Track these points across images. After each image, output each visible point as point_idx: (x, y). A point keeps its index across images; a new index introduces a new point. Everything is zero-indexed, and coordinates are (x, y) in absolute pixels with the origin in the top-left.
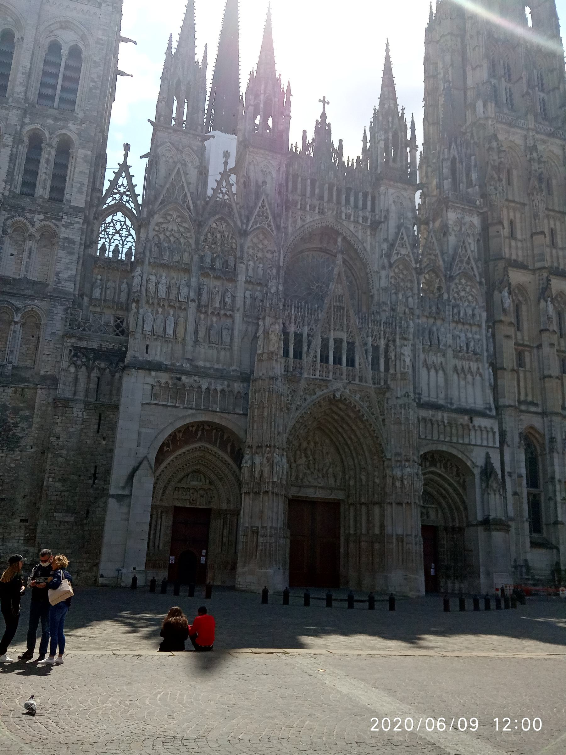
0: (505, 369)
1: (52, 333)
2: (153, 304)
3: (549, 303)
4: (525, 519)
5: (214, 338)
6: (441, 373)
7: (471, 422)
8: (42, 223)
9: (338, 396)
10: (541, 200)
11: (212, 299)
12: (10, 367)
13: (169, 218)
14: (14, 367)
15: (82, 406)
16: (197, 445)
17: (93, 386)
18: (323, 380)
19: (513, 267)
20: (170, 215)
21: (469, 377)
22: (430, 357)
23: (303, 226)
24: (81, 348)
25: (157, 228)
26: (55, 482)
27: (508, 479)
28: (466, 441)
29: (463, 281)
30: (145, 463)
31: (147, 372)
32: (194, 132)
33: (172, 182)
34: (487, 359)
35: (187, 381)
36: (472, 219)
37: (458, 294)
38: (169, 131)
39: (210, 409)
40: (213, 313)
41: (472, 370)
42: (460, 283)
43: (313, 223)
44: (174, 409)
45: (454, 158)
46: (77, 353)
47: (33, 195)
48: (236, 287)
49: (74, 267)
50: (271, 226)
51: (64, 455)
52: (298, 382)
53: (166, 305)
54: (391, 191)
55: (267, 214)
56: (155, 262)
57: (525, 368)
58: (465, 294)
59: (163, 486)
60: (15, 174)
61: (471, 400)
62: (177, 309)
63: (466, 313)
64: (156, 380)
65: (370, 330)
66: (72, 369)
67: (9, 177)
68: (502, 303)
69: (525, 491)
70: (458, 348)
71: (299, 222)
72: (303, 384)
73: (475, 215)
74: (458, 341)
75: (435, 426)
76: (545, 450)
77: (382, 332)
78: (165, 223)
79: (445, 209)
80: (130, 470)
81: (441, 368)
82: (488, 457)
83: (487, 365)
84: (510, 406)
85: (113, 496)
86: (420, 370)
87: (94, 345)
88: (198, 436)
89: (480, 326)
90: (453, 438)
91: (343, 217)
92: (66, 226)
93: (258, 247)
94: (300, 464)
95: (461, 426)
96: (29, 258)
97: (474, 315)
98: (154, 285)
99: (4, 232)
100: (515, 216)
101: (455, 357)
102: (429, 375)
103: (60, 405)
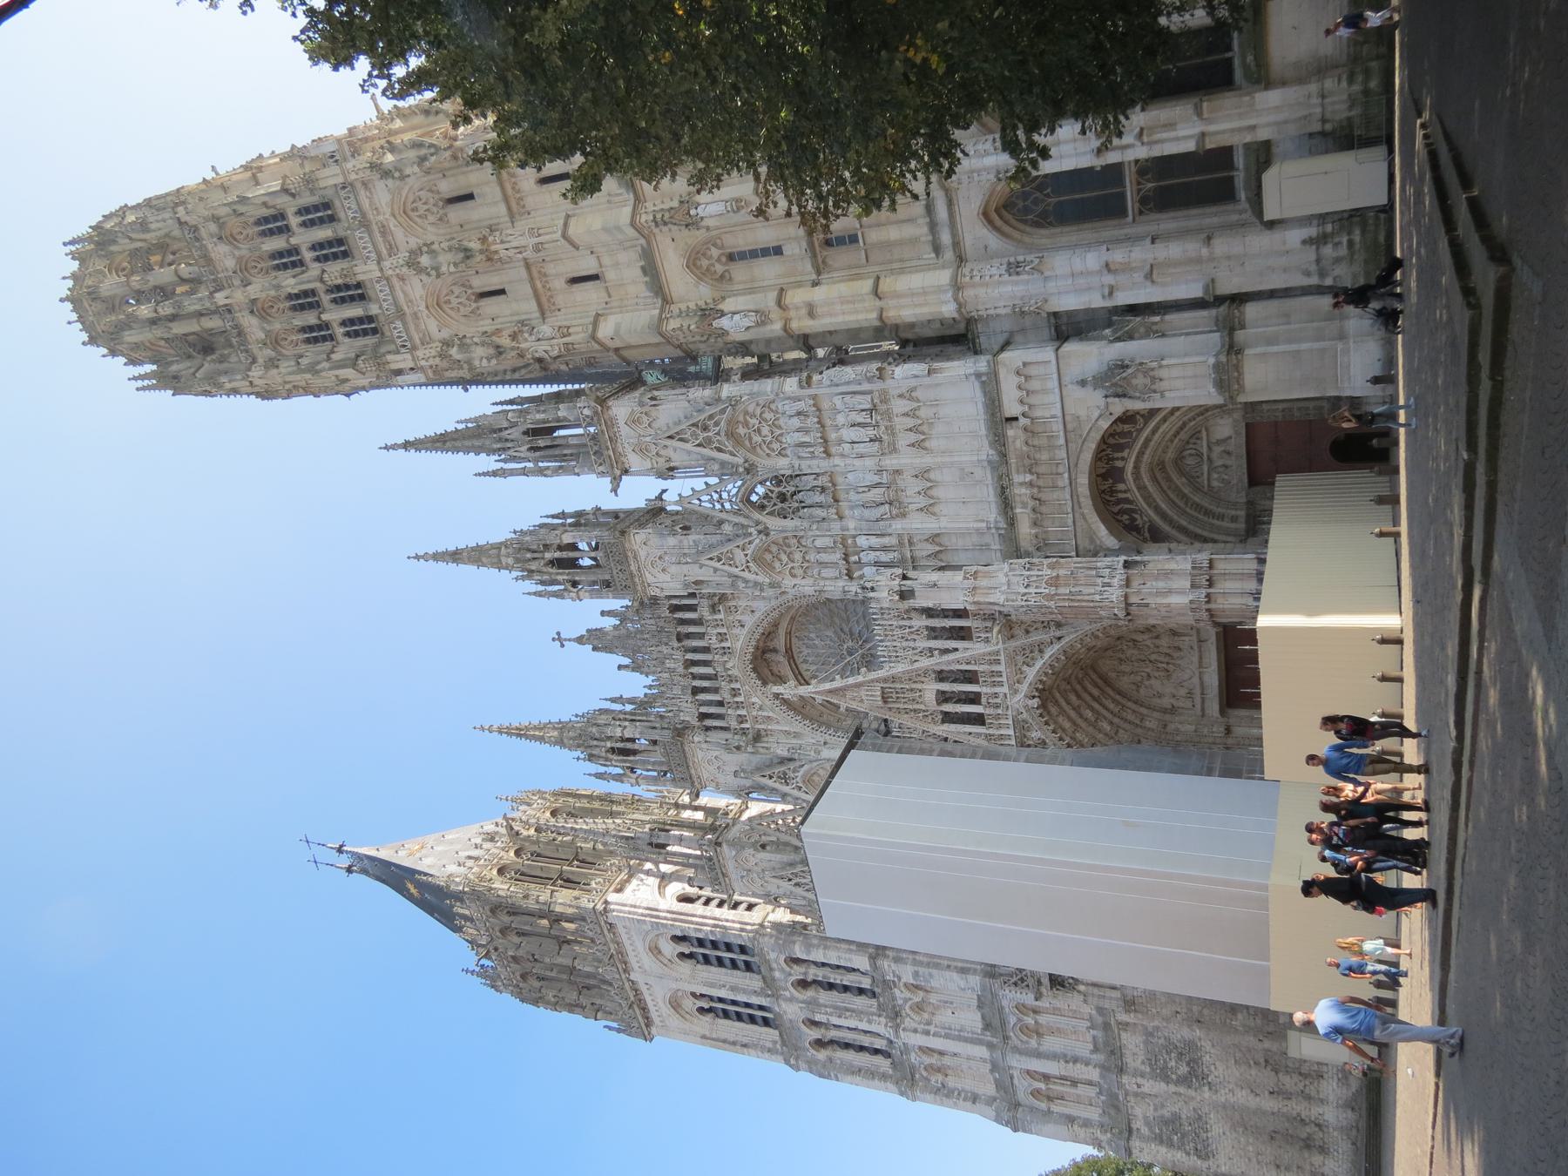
0: (882, 310)
10: (502, 242)
12: (1095, 1032)
22: (910, 500)
28: (1057, 427)
29: (741, 431)
37: (771, 442)
41: (907, 409)
43: (759, 693)
45: (531, 449)
49: (948, 974)
54: (649, 578)
65: (905, 644)
74: (860, 448)
81: (926, 475)
82: (1083, 383)
83: (889, 382)
86: (943, 525)
89: (814, 397)
97: (799, 414)
99: (929, 1023)
101: (893, 449)
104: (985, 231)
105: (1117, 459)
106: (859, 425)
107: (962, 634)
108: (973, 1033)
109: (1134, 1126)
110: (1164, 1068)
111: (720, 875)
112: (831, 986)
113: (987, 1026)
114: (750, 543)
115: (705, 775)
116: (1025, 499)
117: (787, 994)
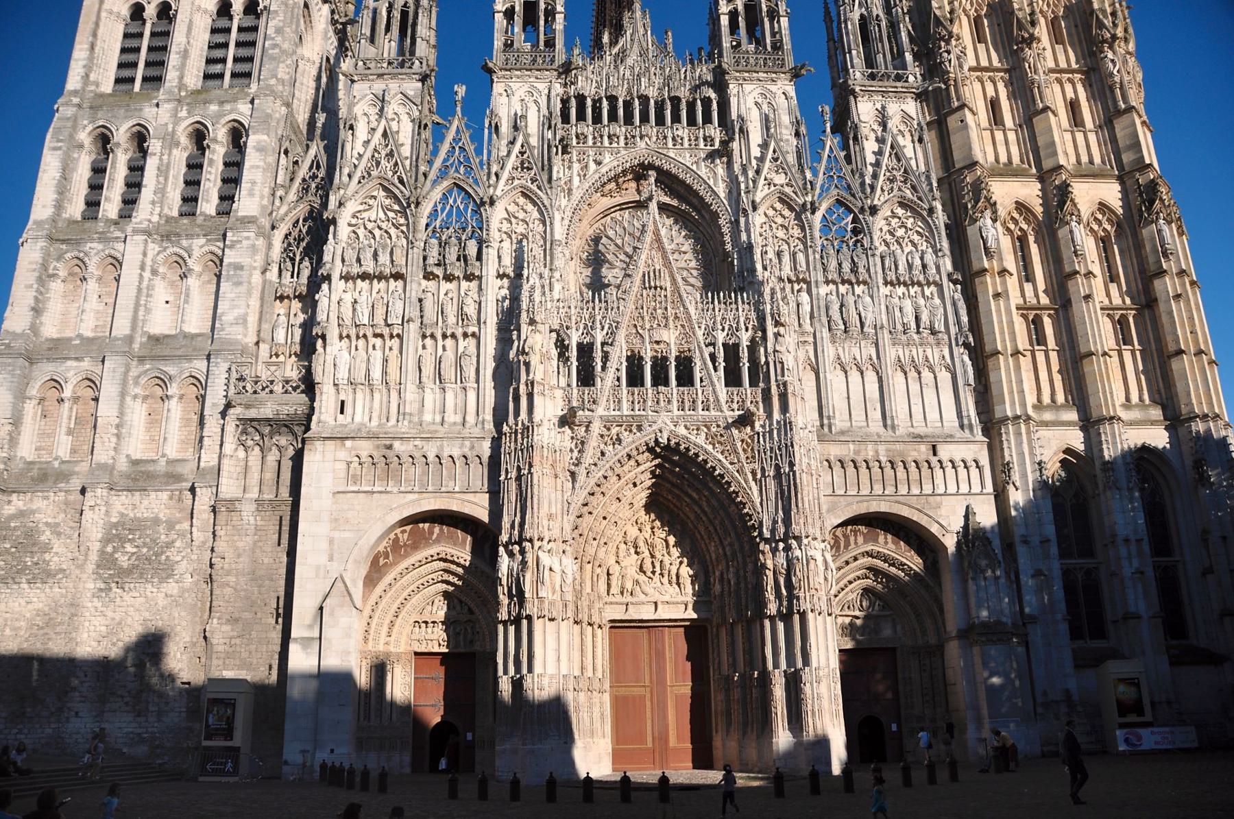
1: (214, 405)
2: (348, 336)
3: (1073, 224)
4: (1059, 617)
5: (449, 372)
6: (871, 377)
7: (935, 454)
8: (203, 250)
9: (664, 441)
11: (442, 312)
12: (163, 462)
13: (371, 202)
14: (171, 462)
15: (253, 507)
16: (433, 551)
17: (270, 475)
18: (632, 416)
19: (1001, 175)
20: (375, 198)
21: (927, 375)
23: (596, 171)
24: (252, 420)
25: (354, 221)
26: (221, 624)
27: (1021, 550)
29: (900, 211)
30: (339, 584)
31: (338, 442)
32: (408, 71)
33: (375, 150)
34: (956, 339)
35: (403, 448)
36: (904, 107)
37: (894, 236)
38: (371, 77)
39: (443, 489)
40: (444, 336)
42: (894, 215)
43: (616, 163)
44: (383, 496)
46: (246, 429)
47: (194, 214)
48: (480, 289)
49: (242, 303)
50: (537, 180)
51: (231, 584)
52: (587, 427)
53: (369, 334)
54: (748, 87)
55: (529, 162)
56: (348, 273)
57: (1047, 346)
58: (906, 233)
59: (387, 621)
60: (169, 190)
61: (933, 415)
62: (387, 337)
63: (910, 266)
64: (354, 453)
65: (719, 319)
66: (241, 454)
67: (159, 195)
68: (982, 237)
69: (1056, 567)
70: (899, 327)
71: (592, 166)
72: (597, 427)
73: (910, 99)
74: (897, 314)
75: (863, 470)
76: (1097, 488)
77: (742, 319)
78: (365, 211)
79: (852, 98)
80: (320, 599)
83: (959, 351)
84: (1017, 418)
85: (295, 639)
86: (828, 375)
87: (267, 411)
88: (435, 536)
90: (875, 487)
91: (670, 144)
92: (231, 247)
93: (516, 218)
94: (626, 567)
95: (913, 464)
96: (186, 302)
97: (924, 266)
98: (349, 305)
99: (154, 272)
100: (996, 91)
102: (847, 382)
103: (223, 509)
104: (1055, 448)
105: (886, 538)
106: (916, 317)
107: (733, 379)
108: (144, 321)
109: (14, 497)
110: (123, 540)
111: (380, 71)
112: (195, 166)
113: (156, 340)
114: (795, 193)
115: (514, 86)
116: (863, 453)
117: (183, 113)
